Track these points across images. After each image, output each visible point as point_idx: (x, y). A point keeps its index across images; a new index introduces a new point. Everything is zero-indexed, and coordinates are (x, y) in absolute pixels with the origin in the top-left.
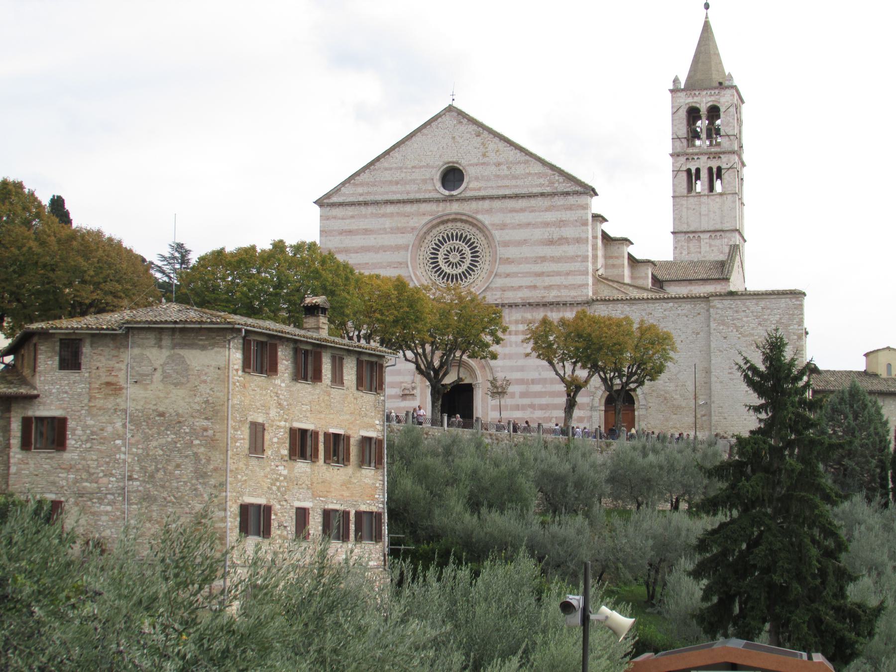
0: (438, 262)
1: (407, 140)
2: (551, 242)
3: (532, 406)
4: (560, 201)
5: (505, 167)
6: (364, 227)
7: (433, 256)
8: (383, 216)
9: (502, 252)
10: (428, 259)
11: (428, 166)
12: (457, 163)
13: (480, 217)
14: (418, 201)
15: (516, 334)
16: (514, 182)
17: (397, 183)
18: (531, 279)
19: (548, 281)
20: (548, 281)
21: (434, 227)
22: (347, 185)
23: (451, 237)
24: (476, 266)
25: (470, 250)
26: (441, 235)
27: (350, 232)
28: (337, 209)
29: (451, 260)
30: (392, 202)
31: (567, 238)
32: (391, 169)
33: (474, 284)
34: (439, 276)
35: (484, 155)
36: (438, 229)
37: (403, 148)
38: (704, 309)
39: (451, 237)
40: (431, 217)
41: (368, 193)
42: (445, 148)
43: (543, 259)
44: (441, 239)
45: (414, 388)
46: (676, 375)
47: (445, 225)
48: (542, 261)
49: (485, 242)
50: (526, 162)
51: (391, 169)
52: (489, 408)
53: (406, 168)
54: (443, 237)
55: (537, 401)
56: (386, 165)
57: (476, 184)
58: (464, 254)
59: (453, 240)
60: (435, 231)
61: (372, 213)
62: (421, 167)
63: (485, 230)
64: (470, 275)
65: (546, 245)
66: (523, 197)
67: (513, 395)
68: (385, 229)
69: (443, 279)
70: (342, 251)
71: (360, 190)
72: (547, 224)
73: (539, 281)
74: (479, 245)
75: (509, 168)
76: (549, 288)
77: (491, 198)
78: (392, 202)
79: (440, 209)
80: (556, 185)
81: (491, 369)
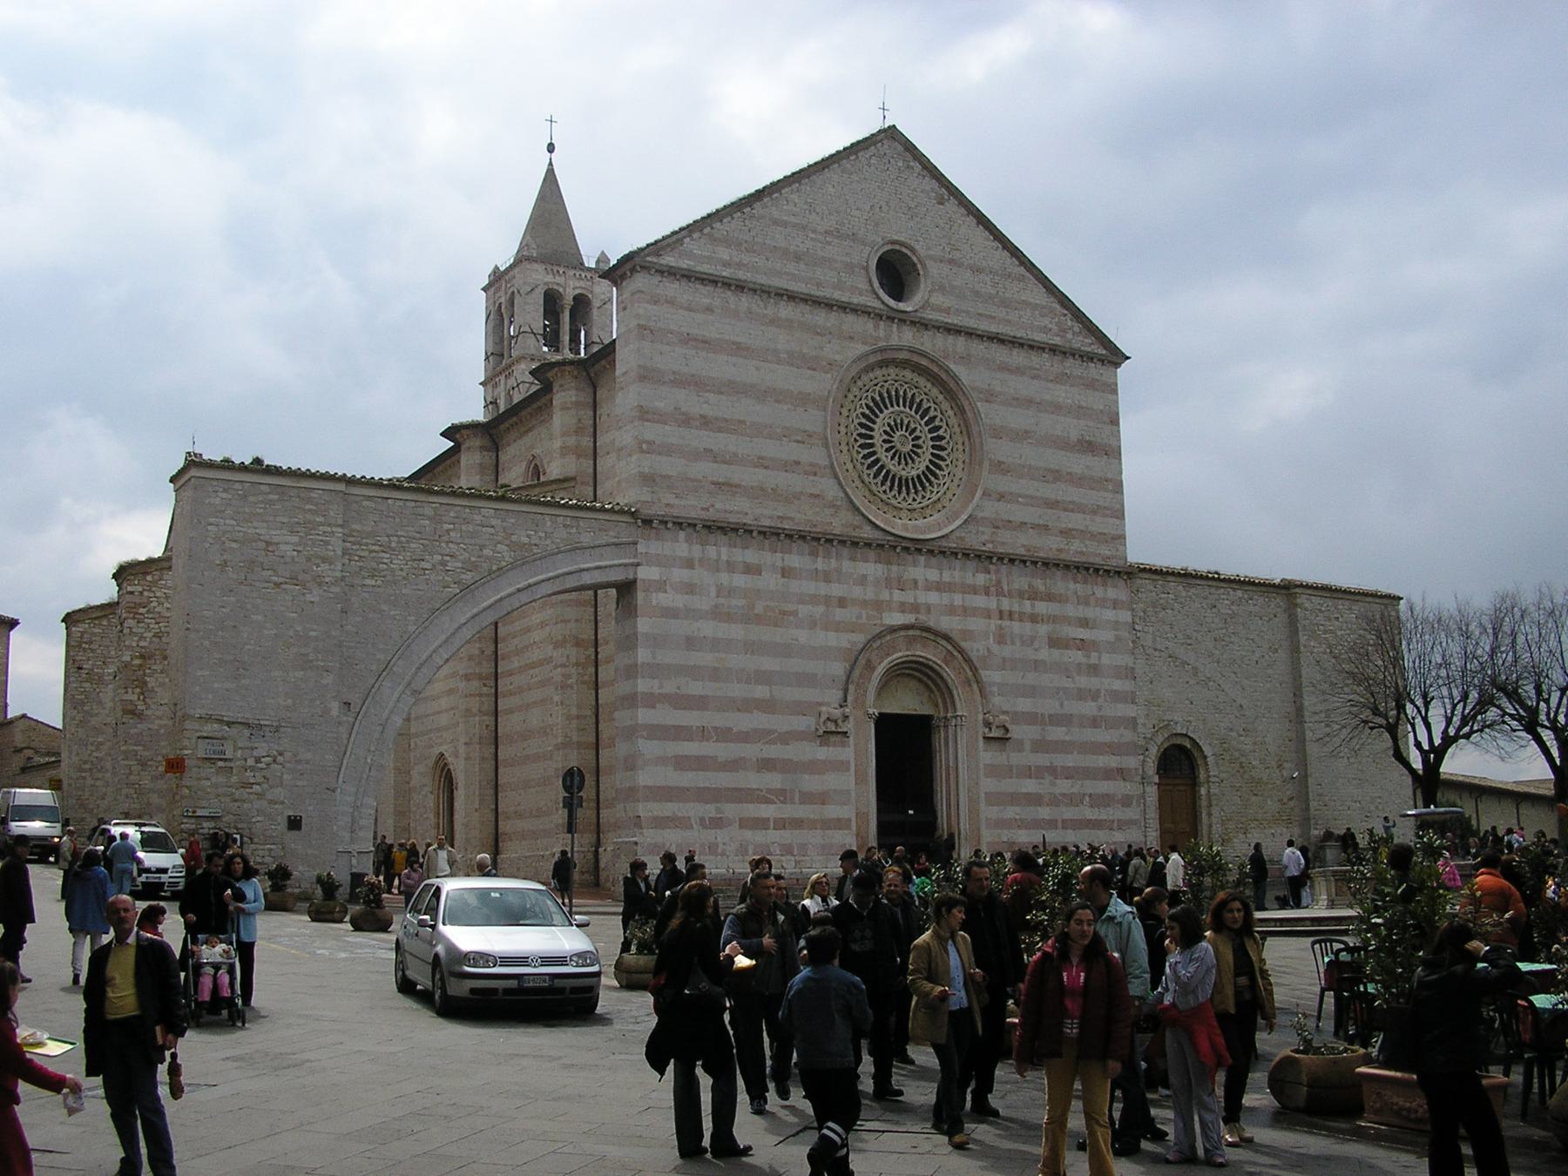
0: (872, 445)
7: (863, 431)
9: (999, 449)
13: (952, 366)
14: (844, 308)
15: (1021, 620)
21: (870, 368)
23: (895, 399)
26: (878, 388)
29: (898, 445)
30: (792, 297)
33: (939, 506)
36: (871, 375)
40: (867, 348)
41: (740, 265)
42: (885, 208)
43: (1056, 476)
47: (884, 371)
48: (1056, 480)
49: (953, 421)
50: (1021, 279)
57: (941, 298)
58: (918, 438)
59: (898, 406)
60: (865, 378)
63: (960, 395)
66: (1022, 345)
72: (1057, 408)
74: (945, 426)
76: (1066, 533)
77: (970, 334)
78: (792, 297)
80: (1069, 336)
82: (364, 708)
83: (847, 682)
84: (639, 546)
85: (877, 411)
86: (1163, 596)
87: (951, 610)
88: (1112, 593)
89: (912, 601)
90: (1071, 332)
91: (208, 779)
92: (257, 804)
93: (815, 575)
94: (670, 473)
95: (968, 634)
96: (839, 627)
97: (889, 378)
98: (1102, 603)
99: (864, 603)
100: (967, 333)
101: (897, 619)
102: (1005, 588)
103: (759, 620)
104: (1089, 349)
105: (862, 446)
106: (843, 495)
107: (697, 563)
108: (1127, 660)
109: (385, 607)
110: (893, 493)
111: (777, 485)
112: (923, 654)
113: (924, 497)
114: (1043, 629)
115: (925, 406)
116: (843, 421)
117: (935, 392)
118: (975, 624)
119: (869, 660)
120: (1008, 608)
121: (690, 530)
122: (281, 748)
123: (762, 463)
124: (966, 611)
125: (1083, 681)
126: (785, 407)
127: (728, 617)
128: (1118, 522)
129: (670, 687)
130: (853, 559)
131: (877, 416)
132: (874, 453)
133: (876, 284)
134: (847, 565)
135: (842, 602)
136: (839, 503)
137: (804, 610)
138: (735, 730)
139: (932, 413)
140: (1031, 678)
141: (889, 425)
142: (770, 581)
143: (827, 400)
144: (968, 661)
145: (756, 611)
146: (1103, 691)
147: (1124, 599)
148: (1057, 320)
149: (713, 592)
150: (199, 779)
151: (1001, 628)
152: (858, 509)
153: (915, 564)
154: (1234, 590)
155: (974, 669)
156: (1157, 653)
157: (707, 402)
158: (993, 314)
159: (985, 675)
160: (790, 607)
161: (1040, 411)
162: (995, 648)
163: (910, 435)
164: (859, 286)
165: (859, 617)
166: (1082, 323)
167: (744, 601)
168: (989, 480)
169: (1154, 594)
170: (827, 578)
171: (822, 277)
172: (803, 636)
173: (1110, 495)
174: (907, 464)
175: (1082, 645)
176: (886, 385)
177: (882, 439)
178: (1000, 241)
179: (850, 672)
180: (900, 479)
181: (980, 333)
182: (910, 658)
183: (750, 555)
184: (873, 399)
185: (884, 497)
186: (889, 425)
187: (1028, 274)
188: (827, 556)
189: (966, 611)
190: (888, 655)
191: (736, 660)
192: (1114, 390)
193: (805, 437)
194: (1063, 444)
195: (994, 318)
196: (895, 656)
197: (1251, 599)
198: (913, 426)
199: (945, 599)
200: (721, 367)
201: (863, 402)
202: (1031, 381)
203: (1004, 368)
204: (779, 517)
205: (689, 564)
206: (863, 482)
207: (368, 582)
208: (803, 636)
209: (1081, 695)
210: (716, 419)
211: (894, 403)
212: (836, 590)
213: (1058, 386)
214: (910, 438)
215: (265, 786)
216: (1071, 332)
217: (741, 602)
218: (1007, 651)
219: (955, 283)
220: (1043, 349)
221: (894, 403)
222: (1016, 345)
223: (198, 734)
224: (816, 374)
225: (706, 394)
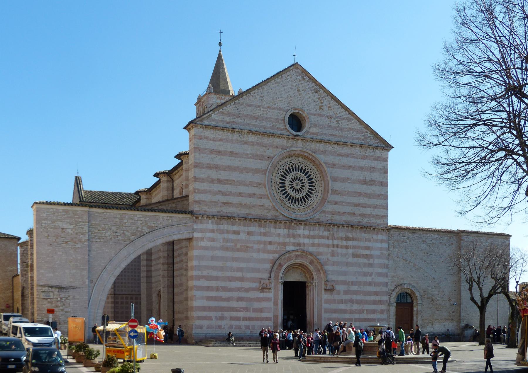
1: (264, 85)
2: (365, 182)
3: (351, 301)
4: (370, 152)
5: (335, 121)
6: (230, 150)
7: (281, 181)
10: (278, 183)
11: (279, 109)
12: (302, 110)
13: (317, 156)
15: (341, 248)
16: (340, 133)
17: (256, 118)
18: (352, 208)
19: (363, 211)
20: (363, 211)
21: (284, 158)
22: (216, 113)
25: (308, 180)
26: (288, 165)
27: (219, 153)
28: (208, 132)
29: (295, 186)
31: (374, 181)
32: (252, 106)
33: (311, 207)
34: (286, 198)
35: (320, 108)
36: (285, 160)
37: (260, 90)
38: (455, 240)
39: (294, 169)
42: (293, 96)
43: (359, 194)
45: (270, 283)
46: (439, 284)
47: (291, 159)
48: (359, 196)
50: (349, 119)
51: (252, 106)
52: (323, 302)
53: (263, 107)
54: (289, 168)
55: (355, 297)
56: (247, 101)
57: (315, 129)
58: (303, 183)
59: (296, 171)
60: (283, 162)
62: (274, 109)
65: (362, 184)
67: (339, 293)
68: (247, 154)
70: (213, 168)
71: (227, 119)
72: (362, 169)
73: (357, 210)
74: (314, 178)
75: (337, 122)
77: (325, 142)
79: (289, 145)
80: (368, 140)
81: (325, 273)
82: (97, 282)
83: (271, 271)
84: (194, 225)
85: (287, 174)
86: (403, 237)
87: (313, 245)
88: (380, 237)
89: (298, 242)
90: (369, 139)
91: (45, 304)
92: (61, 313)
93: (261, 234)
94: (206, 200)
95: (320, 254)
96: (269, 252)
97: (292, 161)
98: (376, 241)
99: (279, 244)
100: (324, 142)
101: (291, 248)
102: (336, 236)
103: (238, 250)
104: (377, 145)
105: (281, 187)
106: (271, 205)
107: (216, 231)
108: (386, 261)
109: (104, 249)
110: (292, 203)
112: (302, 261)
113: (305, 204)
114: (350, 251)
115: (307, 171)
116: (273, 178)
117: (311, 165)
118: (321, 250)
119: (280, 263)
120: (336, 244)
121: (213, 219)
122: (69, 295)
123: (241, 195)
124: (319, 245)
125: (366, 270)
127: (226, 249)
128: (385, 210)
129: (205, 273)
130: (275, 228)
131: (287, 176)
132: (285, 189)
133: (288, 126)
134: (273, 230)
135: (270, 243)
136: (270, 208)
137: (256, 246)
138: (229, 288)
139: (309, 173)
140: (344, 269)
141: (292, 179)
142: (243, 236)
143: (266, 171)
144: (319, 263)
145: (237, 247)
146: (374, 274)
147: (386, 239)
148: (363, 134)
149: (222, 241)
150: (42, 305)
151: (333, 251)
152: (277, 210)
153: (299, 229)
154: (434, 234)
155: (322, 265)
156: (398, 259)
157: (220, 174)
158: (336, 134)
159: (327, 268)
160: (250, 245)
162: (330, 258)
163: (300, 182)
164: (281, 127)
165: (277, 248)
166: (374, 135)
167: (233, 244)
168: (331, 197)
169: (398, 237)
170: (265, 235)
171: (266, 125)
172: (255, 255)
173: (382, 201)
174: (298, 193)
175: (367, 256)
176: (291, 164)
178: (341, 105)
179: (273, 267)
181: (330, 142)
182: (296, 262)
183: (235, 228)
184: (286, 170)
185: (289, 205)
186: (292, 179)
187: (352, 117)
188: (265, 227)
189: (319, 245)
190: (288, 261)
191: (229, 264)
192: (386, 160)
193: (258, 185)
194: (365, 182)
195: (337, 135)
196: (290, 262)
197: (441, 238)
198: (301, 178)
199: (310, 241)
200: (226, 161)
201: (282, 170)
203: (340, 155)
204: (247, 214)
205: (213, 231)
206: (280, 200)
207: (99, 240)
208: (255, 255)
209: (365, 274)
210: (224, 180)
211: (294, 170)
212: (269, 239)
213: (362, 160)
214: (300, 183)
215: (64, 307)
216: (369, 139)
217: (231, 244)
218: (335, 259)
219: (320, 123)
220: (357, 146)
221: (294, 170)
222: (345, 145)
223: (41, 291)
225: (221, 172)
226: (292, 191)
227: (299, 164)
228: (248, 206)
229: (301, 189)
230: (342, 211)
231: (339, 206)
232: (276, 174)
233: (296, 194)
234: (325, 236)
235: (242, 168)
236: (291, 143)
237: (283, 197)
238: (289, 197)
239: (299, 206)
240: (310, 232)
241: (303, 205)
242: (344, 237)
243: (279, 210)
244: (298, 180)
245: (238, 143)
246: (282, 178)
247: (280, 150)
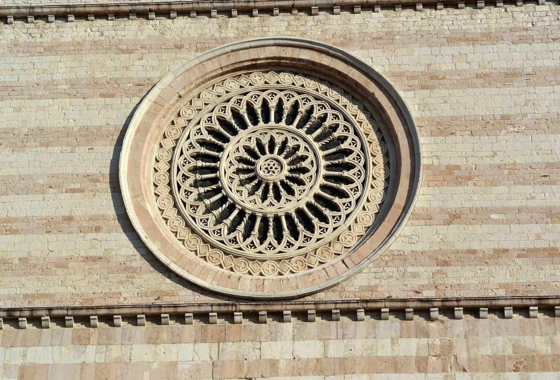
7: (200, 163)
8: (50, 49)
10: (184, 170)
18: (538, 228)
24: (343, 195)
29: (261, 173)
33: (338, 247)
36: (220, 90)
44: (228, 116)
47: (243, 81)
59: (267, 120)
61: (16, 45)
64: (324, 219)
68: (51, 84)
69: (232, 229)
79: (231, 33)
111: (29, 253)
126: (57, 149)
130: (153, 341)
136: (134, 264)
161: (535, 85)
176: (245, 98)
177: (233, 168)
180: (265, 220)
185: (230, 247)
198: (291, 144)
202: (513, 47)
204: (26, 296)
206: (193, 231)
224: (116, 101)
226: (245, 192)
227: (281, 95)
228: (35, 266)
229: (290, 183)
230: (489, 246)
231: (470, 228)
232: (177, 140)
233: (267, 202)
234: (407, 358)
235: (26, 130)
236: (237, 29)
237: (205, 222)
238: (232, 217)
239: (281, 247)
240: (325, 347)
241: (297, 244)
242: (510, 358)
243: (173, 267)
244: (276, 150)
245: (21, 54)
246: (203, 150)
247: (193, 55)
